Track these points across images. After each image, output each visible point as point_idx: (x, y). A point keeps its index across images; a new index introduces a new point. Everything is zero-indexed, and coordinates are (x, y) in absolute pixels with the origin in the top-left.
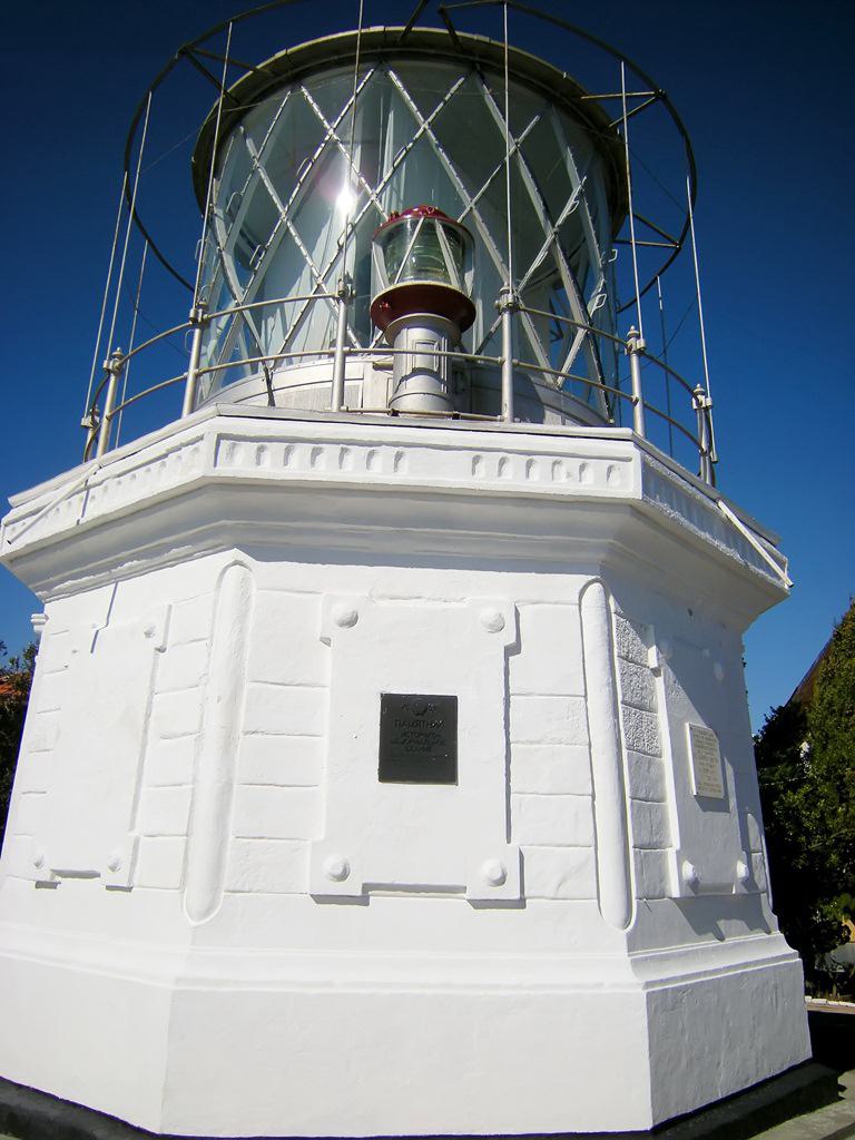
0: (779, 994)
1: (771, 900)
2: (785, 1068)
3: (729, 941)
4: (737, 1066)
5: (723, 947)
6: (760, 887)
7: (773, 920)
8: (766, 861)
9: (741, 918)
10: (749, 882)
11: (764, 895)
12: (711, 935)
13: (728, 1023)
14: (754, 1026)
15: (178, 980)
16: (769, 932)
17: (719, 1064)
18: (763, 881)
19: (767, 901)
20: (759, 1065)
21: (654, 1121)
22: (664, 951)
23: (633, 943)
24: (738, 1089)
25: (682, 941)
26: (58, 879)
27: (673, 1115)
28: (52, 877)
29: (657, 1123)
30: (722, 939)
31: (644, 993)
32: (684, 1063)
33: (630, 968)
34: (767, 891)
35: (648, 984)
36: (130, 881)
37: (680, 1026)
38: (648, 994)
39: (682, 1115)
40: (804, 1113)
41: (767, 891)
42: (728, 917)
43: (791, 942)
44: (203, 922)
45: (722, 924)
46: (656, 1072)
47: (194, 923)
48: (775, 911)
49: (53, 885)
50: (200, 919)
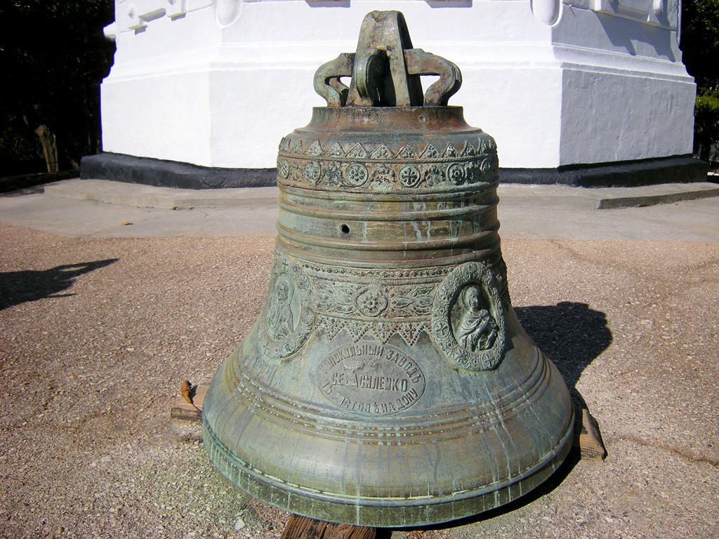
0: (674, 103)
1: (679, 38)
2: (670, 155)
3: (637, 57)
4: (632, 143)
5: (634, 60)
6: (671, 25)
7: (679, 54)
8: (680, 7)
9: (651, 43)
10: (662, 15)
11: (673, 33)
12: (625, 48)
13: (630, 111)
14: (650, 119)
15: (213, 65)
16: (673, 61)
17: (618, 137)
18: (675, 22)
19: (675, 40)
20: (651, 147)
21: (561, 163)
22: (583, 49)
23: (556, 36)
24: (631, 158)
25: (600, 47)
26: (145, 23)
27: (577, 162)
28: (141, 23)
29: (562, 165)
30: (633, 54)
31: (562, 70)
32: (590, 128)
33: (553, 53)
34: (677, 30)
35: (564, 65)
36: (183, 8)
37: (589, 102)
38: (563, 71)
39: (583, 164)
40: (678, 182)
41: (677, 30)
42: (641, 39)
43: (690, 71)
44: (228, 26)
45: (635, 43)
46: (564, 134)
47: (223, 27)
48: (681, 47)
49: (143, 29)
50: (226, 24)
